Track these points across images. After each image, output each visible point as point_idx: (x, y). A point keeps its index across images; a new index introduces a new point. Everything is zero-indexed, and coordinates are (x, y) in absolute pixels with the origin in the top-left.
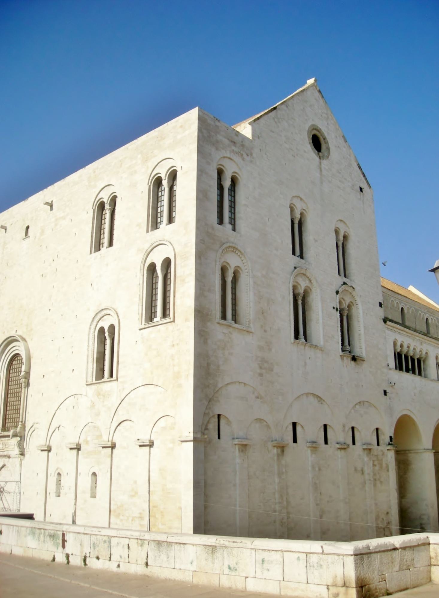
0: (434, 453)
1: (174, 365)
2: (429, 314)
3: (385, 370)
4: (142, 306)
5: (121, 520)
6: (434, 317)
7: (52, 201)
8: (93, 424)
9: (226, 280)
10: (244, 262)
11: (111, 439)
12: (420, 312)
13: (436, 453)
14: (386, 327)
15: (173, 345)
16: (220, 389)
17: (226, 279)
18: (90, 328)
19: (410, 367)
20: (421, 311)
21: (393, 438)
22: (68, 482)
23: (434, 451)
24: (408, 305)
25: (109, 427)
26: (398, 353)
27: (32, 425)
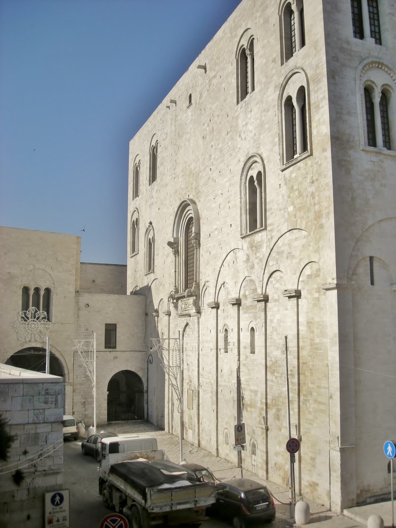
1: (315, 204)
4: (283, 145)
5: (276, 377)
7: (205, 64)
8: (250, 278)
9: (374, 102)
10: (394, 78)
11: (264, 292)
15: (313, 182)
16: (370, 226)
17: (373, 100)
18: (241, 179)
22: (233, 338)
25: (261, 280)
27: (204, 284)
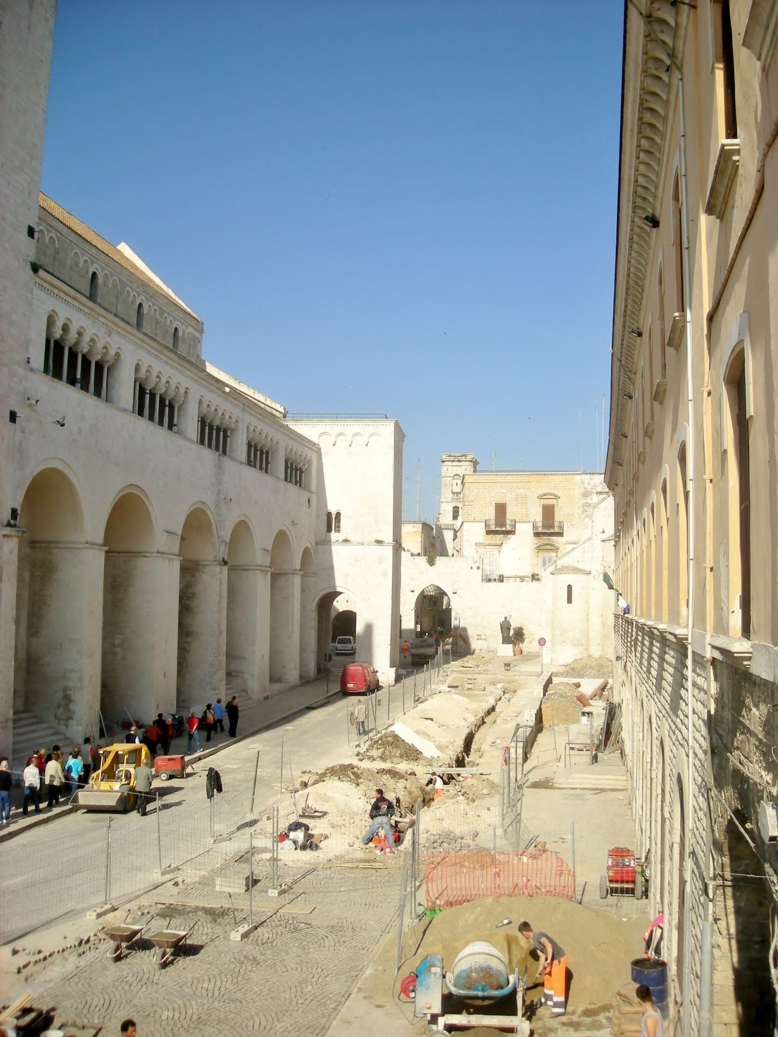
0: (106, 552)
2: (145, 297)
3: (21, 371)
6: (154, 304)
12: (128, 289)
13: (110, 554)
14: (36, 282)
19: (79, 376)
20: (131, 288)
21: (19, 512)
23: (107, 548)
24: (108, 271)
26: (56, 342)
